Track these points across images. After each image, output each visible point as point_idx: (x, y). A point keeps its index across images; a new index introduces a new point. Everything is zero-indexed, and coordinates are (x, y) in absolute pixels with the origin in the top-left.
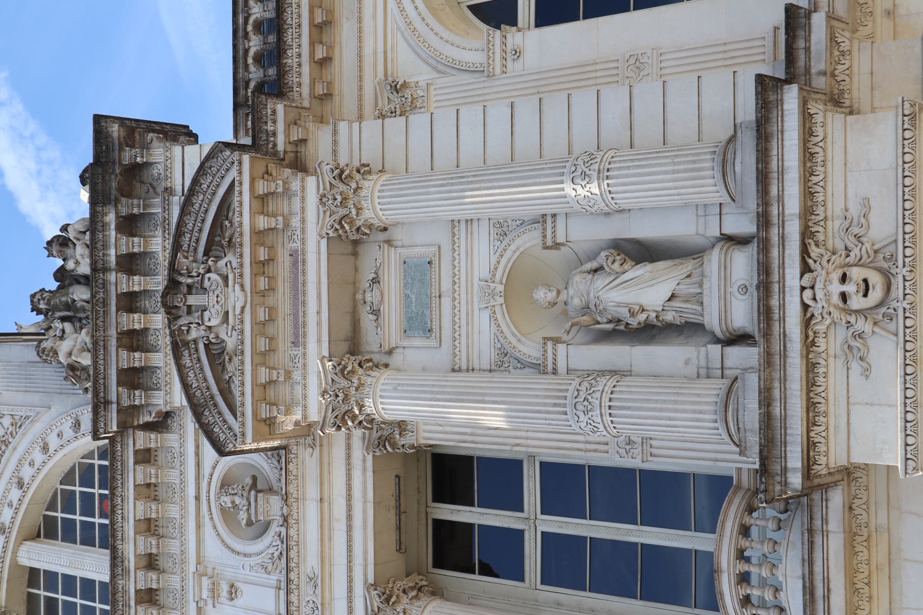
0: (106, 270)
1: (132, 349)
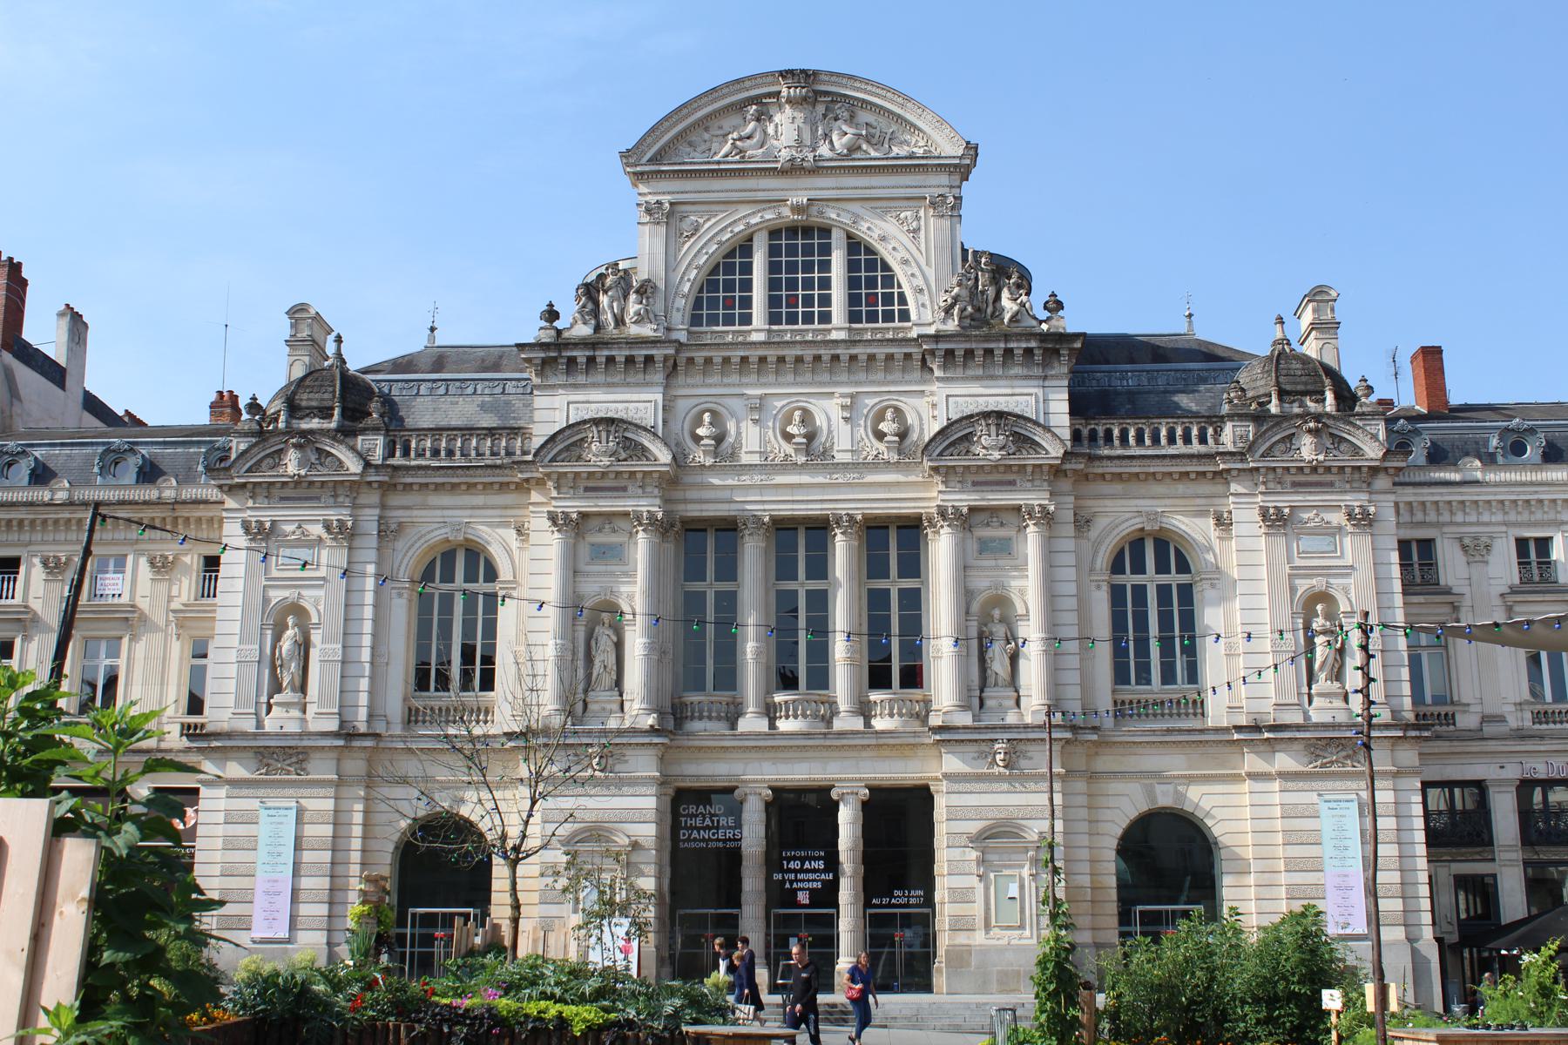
0: (1006, 341)
1: (965, 356)
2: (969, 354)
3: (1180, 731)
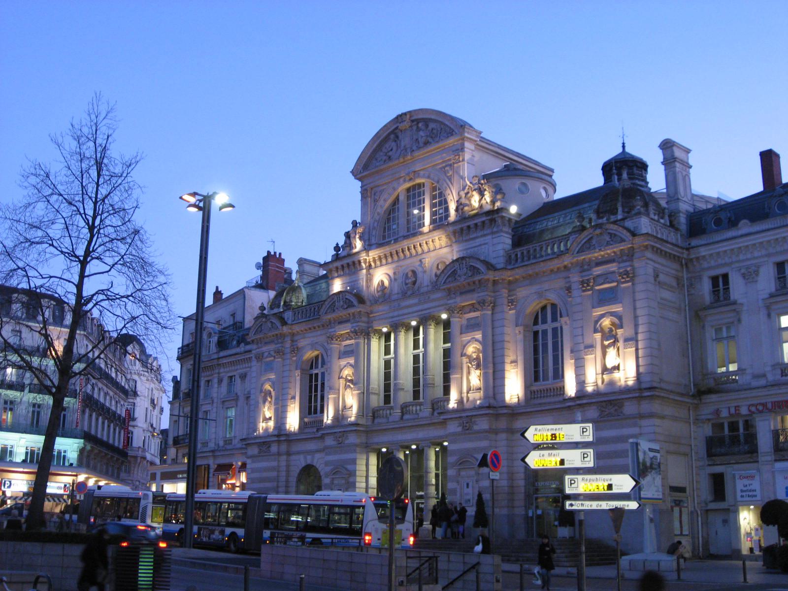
2: (462, 229)
3: (549, 403)
